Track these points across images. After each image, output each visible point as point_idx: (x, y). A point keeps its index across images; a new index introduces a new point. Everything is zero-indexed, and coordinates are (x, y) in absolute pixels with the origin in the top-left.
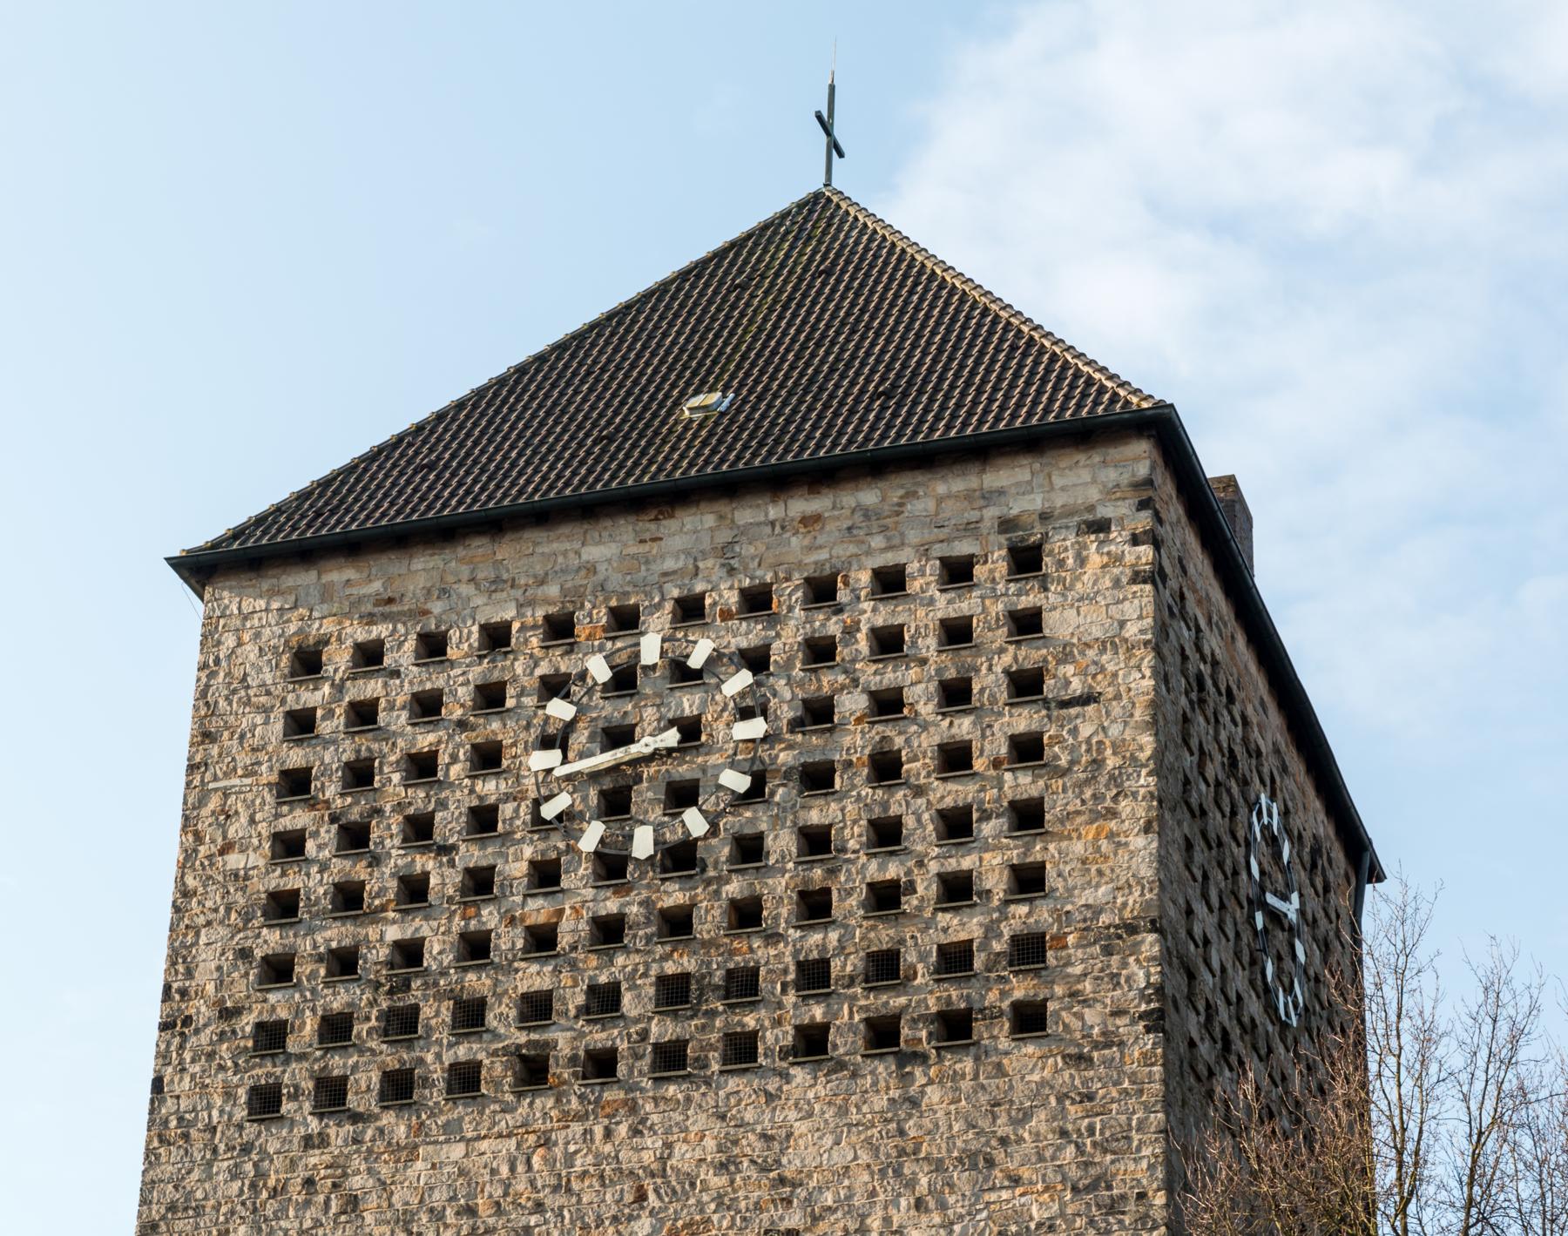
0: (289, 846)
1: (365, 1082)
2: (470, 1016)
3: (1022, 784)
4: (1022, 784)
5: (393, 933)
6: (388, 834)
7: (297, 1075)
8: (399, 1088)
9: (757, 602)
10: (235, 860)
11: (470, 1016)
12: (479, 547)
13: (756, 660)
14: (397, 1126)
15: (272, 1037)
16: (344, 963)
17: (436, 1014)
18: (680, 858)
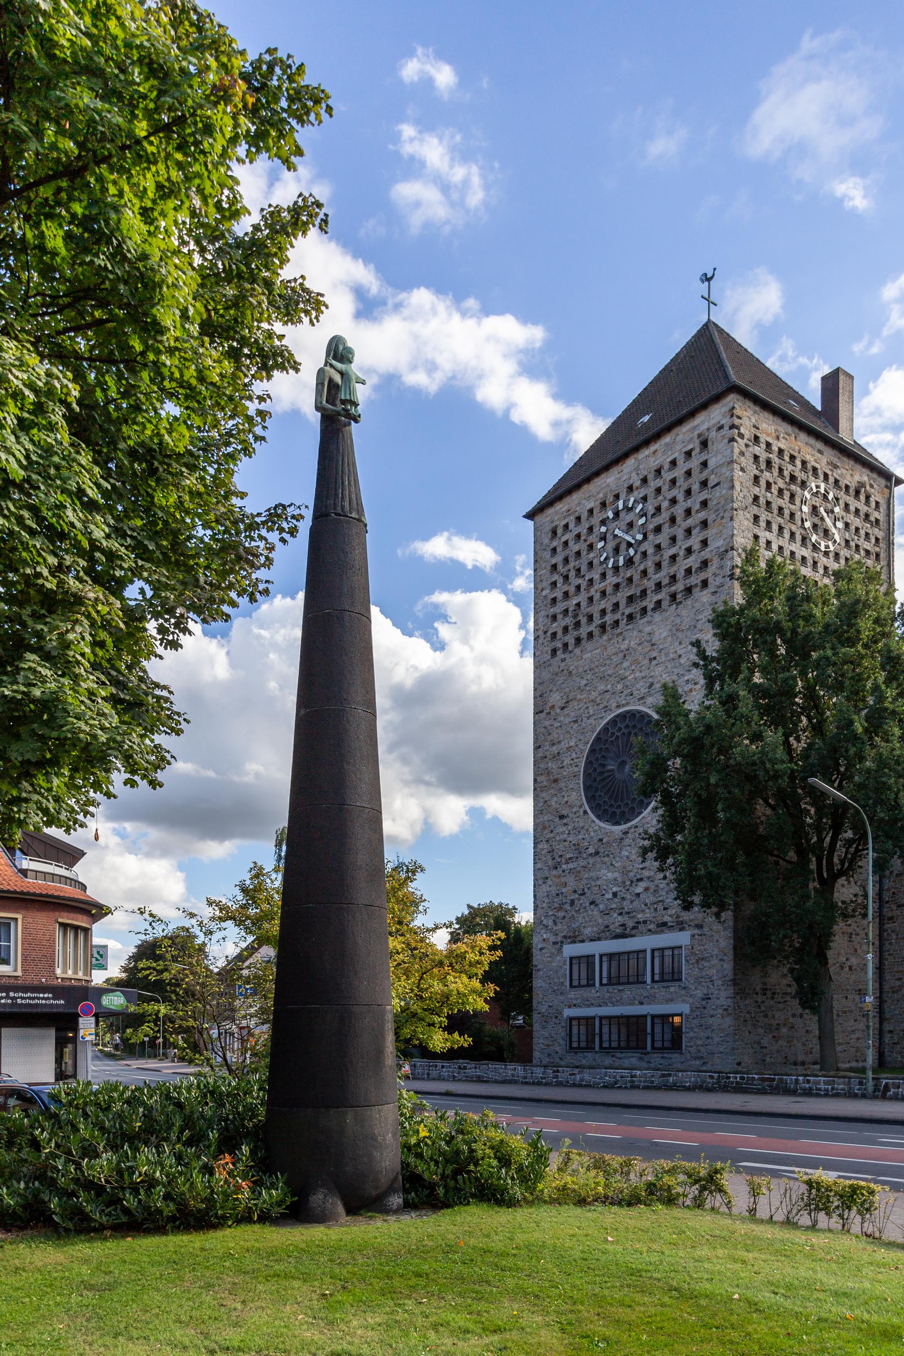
0: (554, 584)
1: (572, 642)
2: (590, 618)
3: (702, 515)
4: (702, 515)
5: (575, 602)
6: (572, 574)
7: (559, 645)
8: (578, 640)
9: (645, 481)
10: (544, 593)
11: (590, 618)
12: (586, 487)
13: (645, 499)
14: (577, 651)
15: (554, 634)
16: (566, 611)
17: (584, 620)
18: (630, 562)
